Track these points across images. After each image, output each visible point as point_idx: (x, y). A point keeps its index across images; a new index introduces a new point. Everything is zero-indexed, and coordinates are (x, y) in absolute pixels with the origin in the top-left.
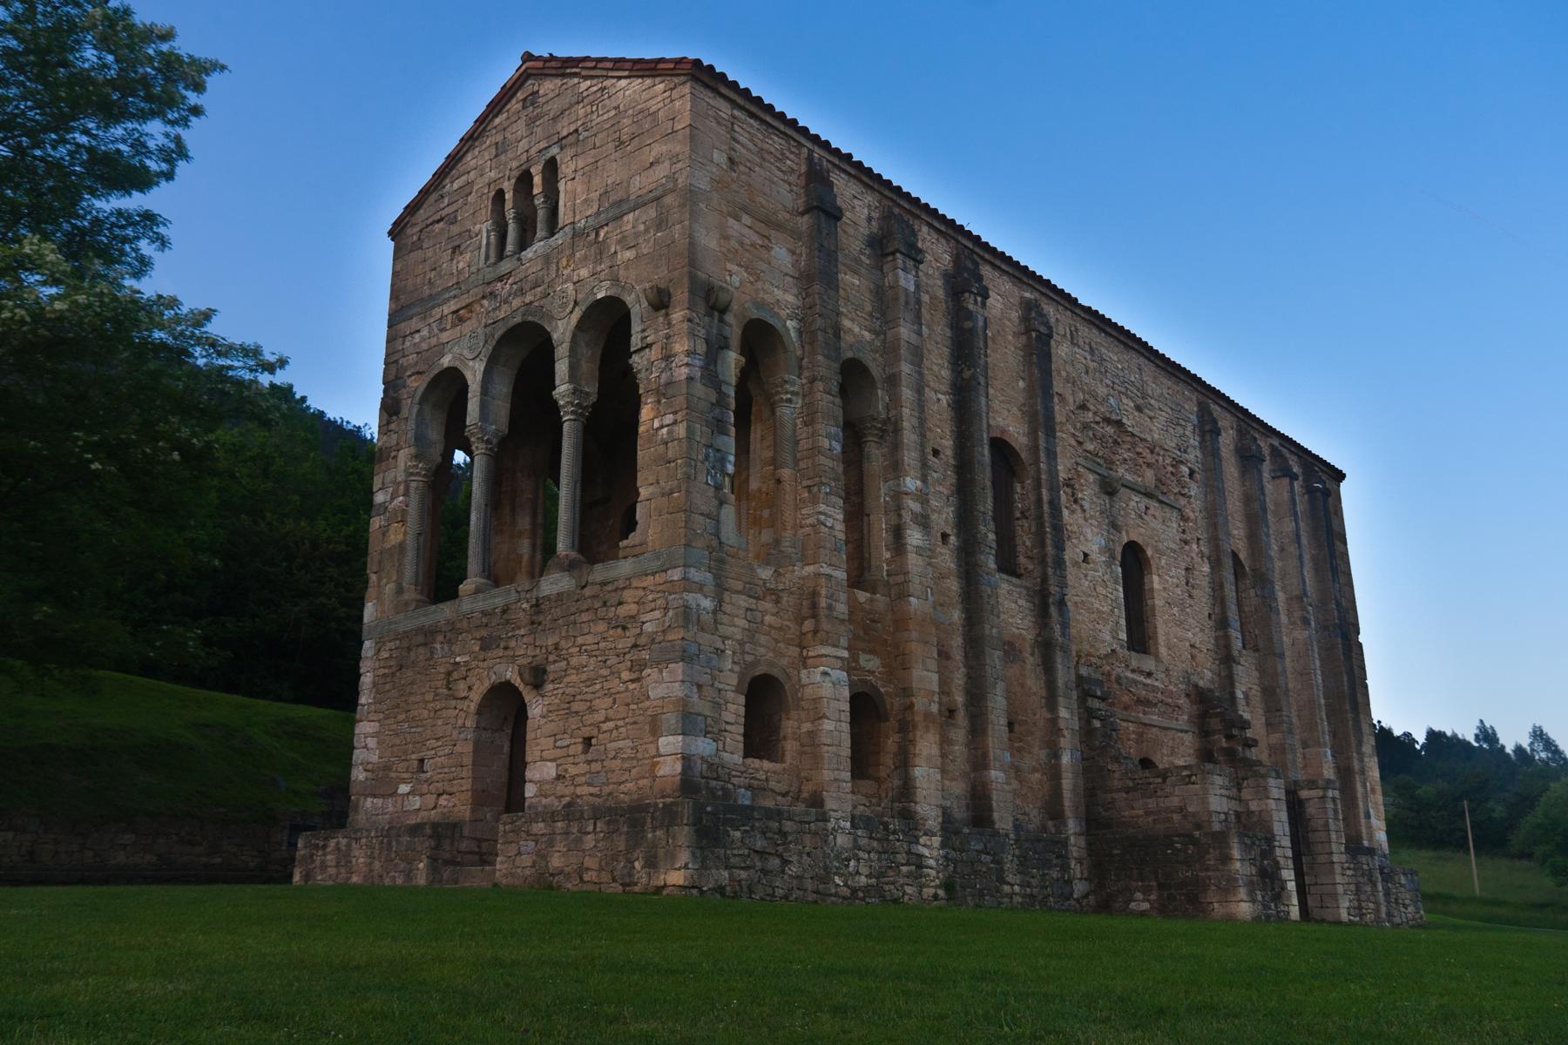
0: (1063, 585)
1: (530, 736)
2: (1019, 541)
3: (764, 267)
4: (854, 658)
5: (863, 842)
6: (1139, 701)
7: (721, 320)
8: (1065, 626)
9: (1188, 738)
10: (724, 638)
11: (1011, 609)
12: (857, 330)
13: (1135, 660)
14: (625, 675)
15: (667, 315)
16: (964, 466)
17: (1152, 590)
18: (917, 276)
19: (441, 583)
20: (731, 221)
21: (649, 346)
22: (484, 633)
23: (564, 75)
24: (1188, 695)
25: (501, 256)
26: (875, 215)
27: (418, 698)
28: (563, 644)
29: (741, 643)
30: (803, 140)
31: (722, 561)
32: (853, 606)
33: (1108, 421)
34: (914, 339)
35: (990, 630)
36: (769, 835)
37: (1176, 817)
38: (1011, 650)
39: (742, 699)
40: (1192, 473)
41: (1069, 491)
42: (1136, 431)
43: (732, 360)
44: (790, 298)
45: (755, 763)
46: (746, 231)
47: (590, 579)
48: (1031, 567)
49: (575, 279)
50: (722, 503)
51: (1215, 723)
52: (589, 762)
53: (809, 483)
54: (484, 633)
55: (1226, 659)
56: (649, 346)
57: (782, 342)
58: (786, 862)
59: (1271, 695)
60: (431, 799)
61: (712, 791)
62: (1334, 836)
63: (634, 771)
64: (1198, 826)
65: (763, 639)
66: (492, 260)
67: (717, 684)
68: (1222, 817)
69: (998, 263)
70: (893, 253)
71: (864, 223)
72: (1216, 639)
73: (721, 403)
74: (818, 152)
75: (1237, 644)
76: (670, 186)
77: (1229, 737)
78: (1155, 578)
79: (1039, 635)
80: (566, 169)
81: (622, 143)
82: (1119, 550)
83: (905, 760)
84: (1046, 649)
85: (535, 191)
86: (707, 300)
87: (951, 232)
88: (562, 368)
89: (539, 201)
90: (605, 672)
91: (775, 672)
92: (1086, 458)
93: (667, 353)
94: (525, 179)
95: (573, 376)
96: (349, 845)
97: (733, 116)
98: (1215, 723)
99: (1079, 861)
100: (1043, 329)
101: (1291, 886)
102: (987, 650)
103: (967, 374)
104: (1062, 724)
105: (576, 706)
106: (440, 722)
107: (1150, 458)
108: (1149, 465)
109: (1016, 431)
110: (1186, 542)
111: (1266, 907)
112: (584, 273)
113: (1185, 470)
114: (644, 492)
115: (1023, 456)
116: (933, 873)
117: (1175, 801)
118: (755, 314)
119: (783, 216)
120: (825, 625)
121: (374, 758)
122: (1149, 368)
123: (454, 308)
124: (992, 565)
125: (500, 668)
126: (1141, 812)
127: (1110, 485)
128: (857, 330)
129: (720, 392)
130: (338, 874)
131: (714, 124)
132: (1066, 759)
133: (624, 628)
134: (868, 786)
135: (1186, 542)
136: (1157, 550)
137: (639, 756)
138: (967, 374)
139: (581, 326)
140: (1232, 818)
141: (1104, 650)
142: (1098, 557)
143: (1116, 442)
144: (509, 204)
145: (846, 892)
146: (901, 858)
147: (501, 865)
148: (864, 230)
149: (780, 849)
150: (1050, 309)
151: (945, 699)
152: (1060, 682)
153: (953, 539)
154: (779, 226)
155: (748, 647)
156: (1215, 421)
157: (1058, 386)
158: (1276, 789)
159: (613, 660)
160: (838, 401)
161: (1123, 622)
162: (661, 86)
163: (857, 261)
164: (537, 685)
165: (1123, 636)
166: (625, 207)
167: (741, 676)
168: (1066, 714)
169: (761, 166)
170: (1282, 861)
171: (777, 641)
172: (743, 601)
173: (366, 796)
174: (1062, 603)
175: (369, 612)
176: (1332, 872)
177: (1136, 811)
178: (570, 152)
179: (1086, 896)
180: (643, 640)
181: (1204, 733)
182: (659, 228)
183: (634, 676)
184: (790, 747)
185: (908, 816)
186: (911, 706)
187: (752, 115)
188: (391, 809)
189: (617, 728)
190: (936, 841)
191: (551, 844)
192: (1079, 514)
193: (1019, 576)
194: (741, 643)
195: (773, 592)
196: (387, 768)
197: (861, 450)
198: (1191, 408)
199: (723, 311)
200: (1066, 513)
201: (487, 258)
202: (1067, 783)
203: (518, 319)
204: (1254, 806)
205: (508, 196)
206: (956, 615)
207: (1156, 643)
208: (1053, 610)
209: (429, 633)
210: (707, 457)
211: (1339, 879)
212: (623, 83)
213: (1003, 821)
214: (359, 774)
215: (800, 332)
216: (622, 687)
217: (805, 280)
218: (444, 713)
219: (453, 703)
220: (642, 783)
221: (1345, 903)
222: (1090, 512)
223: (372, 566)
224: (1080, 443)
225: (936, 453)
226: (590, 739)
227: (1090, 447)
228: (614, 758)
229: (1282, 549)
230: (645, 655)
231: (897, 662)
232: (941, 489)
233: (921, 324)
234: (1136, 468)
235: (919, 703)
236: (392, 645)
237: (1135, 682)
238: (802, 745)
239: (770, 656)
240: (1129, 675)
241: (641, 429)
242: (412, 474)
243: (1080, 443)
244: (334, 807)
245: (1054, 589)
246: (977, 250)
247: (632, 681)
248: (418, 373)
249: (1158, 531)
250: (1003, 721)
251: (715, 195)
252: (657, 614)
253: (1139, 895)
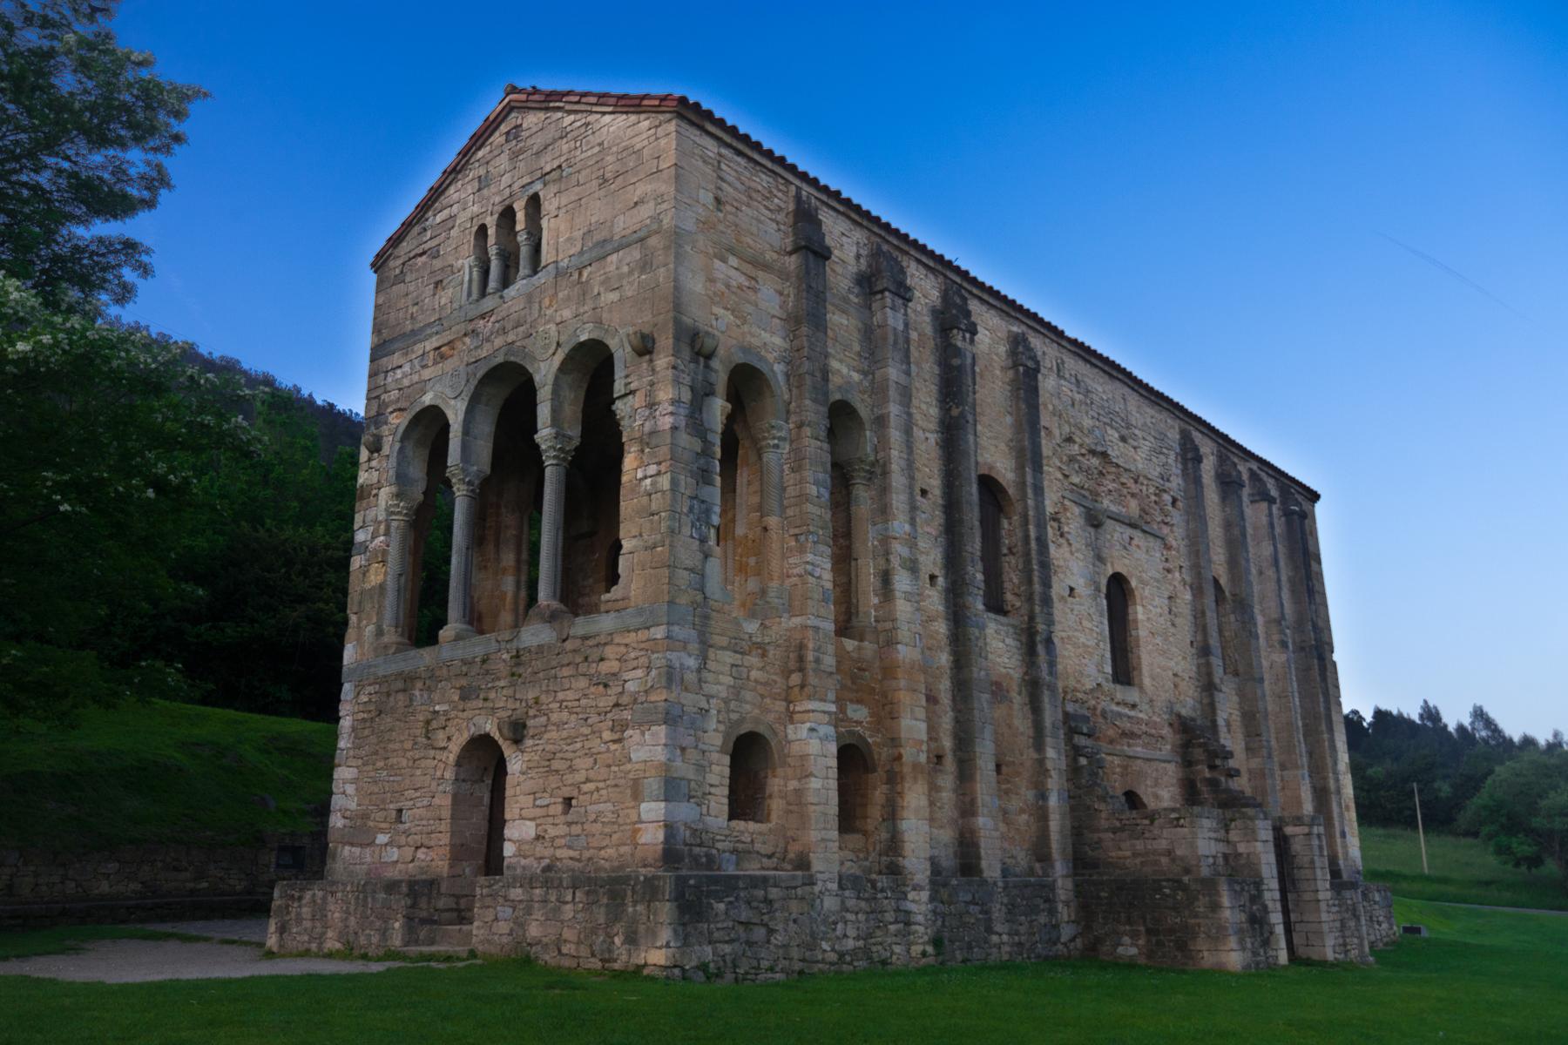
0: (1050, 622)
1: (509, 792)
2: (1005, 577)
3: (750, 308)
4: (842, 709)
5: (851, 903)
6: (1124, 734)
7: (707, 366)
8: (1052, 664)
9: (1171, 768)
10: (709, 697)
11: (998, 647)
12: (845, 371)
13: (1120, 692)
14: (607, 735)
15: (651, 361)
16: (951, 506)
17: (1136, 621)
18: (906, 314)
19: (423, 625)
20: (717, 263)
21: (632, 392)
22: (463, 682)
23: (547, 109)
24: (1171, 725)
25: (483, 293)
26: (864, 252)
27: (397, 746)
28: (543, 698)
29: (726, 701)
30: (790, 177)
31: (706, 617)
32: (841, 656)
33: (1093, 452)
34: (903, 379)
35: (977, 674)
36: (755, 904)
37: (1164, 860)
38: (998, 691)
39: (727, 760)
40: (1174, 501)
41: (1055, 525)
42: (1120, 462)
43: (718, 408)
44: (777, 341)
45: (739, 825)
46: (733, 273)
47: (572, 632)
48: (1018, 604)
49: (558, 320)
50: (706, 556)
51: (1198, 753)
52: (569, 824)
53: (797, 531)
54: (463, 682)
55: (1209, 687)
56: (632, 392)
57: (769, 386)
58: (771, 931)
59: (1251, 720)
60: (408, 852)
61: (695, 859)
62: (1319, 872)
63: (615, 837)
64: (1187, 871)
65: (748, 695)
66: (475, 296)
67: (701, 746)
68: (1211, 860)
69: (985, 297)
70: (882, 292)
71: (852, 261)
72: (1198, 666)
73: (706, 452)
74: (807, 189)
75: (1218, 672)
76: (655, 227)
77: (1212, 767)
78: (1139, 609)
79: (1026, 673)
80: (549, 206)
81: (606, 181)
82: (1104, 582)
83: (892, 813)
84: (1033, 687)
85: (518, 228)
86: (692, 344)
87: (939, 267)
88: (544, 412)
89: (522, 238)
90: (586, 731)
91: (761, 729)
92: (1072, 491)
93: (650, 403)
94: (508, 215)
95: (556, 421)
96: (324, 898)
97: (720, 155)
98: (1198, 753)
99: (1067, 903)
100: (1030, 364)
101: (1280, 929)
102: (976, 694)
103: (955, 412)
104: (1049, 765)
105: (556, 765)
106: (418, 772)
107: (1134, 488)
108: (1133, 495)
109: (1003, 467)
110: (1169, 571)
111: (1255, 954)
112: (567, 314)
113: (1167, 498)
114: (627, 545)
115: (1011, 491)
116: (921, 929)
117: (1163, 844)
118: (740, 358)
119: (770, 256)
120: (813, 679)
121: (353, 806)
122: (1133, 399)
123: (436, 345)
124: (980, 607)
125: (479, 720)
126: (1128, 853)
127: (1096, 518)
128: (845, 371)
129: (705, 441)
130: (314, 927)
131: (700, 163)
132: (1053, 801)
133: (606, 686)
134: (855, 840)
135: (1169, 571)
136: (1141, 581)
137: (621, 821)
138: (955, 412)
139: (562, 369)
140: (1221, 861)
141: (1089, 685)
142: (1082, 588)
143: (1101, 473)
144: (491, 240)
145: (833, 957)
146: (890, 917)
147: (477, 929)
148: (853, 268)
149: (766, 918)
150: (1036, 342)
151: (933, 745)
152: (1048, 722)
153: (941, 581)
154: (766, 267)
155: (733, 705)
156: (1196, 449)
157: (1045, 420)
158: (1265, 832)
159: (594, 719)
160: (826, 446)
161: (1108, 655)
162: (646, 123)
163: (846, 300)
164: (517, 741)
165: (1108, 669)
166: (609, 247)
167: (726, 736)
168: (1054, 755)
169: (748, 205)
170: (1270, 905)
171: (762, 697)
172: (728, 657)
174: (1049, 642)
175: (349, 654)
176: (1318, 910)
177: (1124, 852)
178: (553, 188)
179: (1073, 939)
180: (624, 700)
181: (1187, 763)
182: (643, 270)
183: (616, 737)
184: (776, 806)
185: (894, 870)
186: (900, 757)
187: (739, 153)
188: (369, 859)
189: (598, 790)
190: (925, 895)
191: (529, 911)
192: (1066, 548)
193: (1005, 613)
194: (726, 701)
195: (759, 646)
196: (365, 816)
197: (849, 494)
198: (1174, 435)
199: (709, 356)
200: (1052, 548)
201: (469, 294)
202: (1054, 824)
203: (500, 359)
204: (1242, 848)
205: (491, 231)
206: (944, 659)
207: (1140, 674)
208: (1040, 649)
209: (409, 680)
210: (691, 509)
211: (1324, 917)
212: (608, 118)
213: (991, 868)
214: (336, 821)
215: (787, 376)
216: (603, 748)
217: (793, 322)
218: (423, 763)
219: (432, 753)
220: (623, 849)
221: (1330, 941)
222: (1075, 545)
223: (352, 606)
224: (1066, 476)
225: (924, 492)
226: (570, 799)
227: (1076, 479)
228: (595, 821)
229: (1261, 573)
230: (627, 715)
231: (886, 712)
232: (928, 529)
233: (909, 363)
234: (1120, 499)
235: (908, 753)
236: (371, 689)
237: (1120, 715)
238: (789, 804)
239: (754, 713)
240: (1115, 708)
241: (624, 479)
242: (393, 513)
243: (1066, 476)
244: (307, 855)
245: (1041, 627)
246: (965, 285)
247: (614, 741)
248: (400, 410)
249: (1142, 562)
250: (992, 766)
251: (701, 237)
252: (639, 673)
253: (1126, 940)
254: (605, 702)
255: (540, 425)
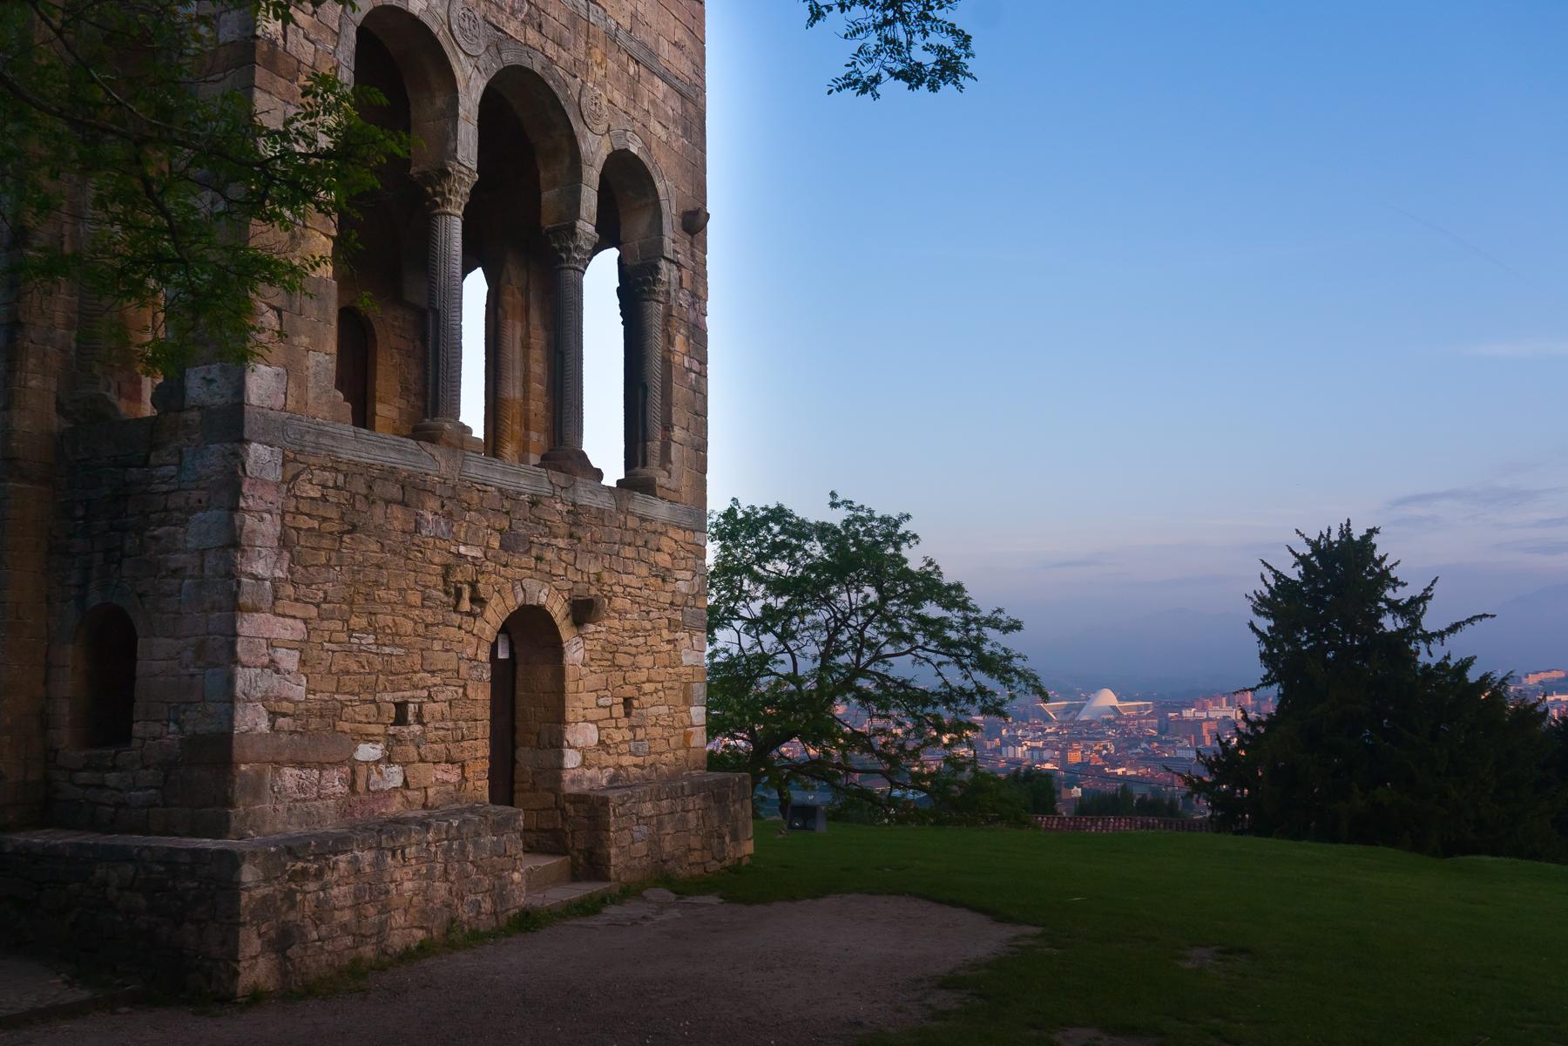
27: (393, 595)
28: (605, 575)
96: (378, 864)
106: (437, 646)
121: (299, 692)
125: (532, 585)
130: (360, 916)
133: (664, 580)
173: (278, 764)
196: (330, 713)
214: (251, 720)
218: (444, 632)
219: (456, 618)
254: (665, 598)
255: (583, 213)
